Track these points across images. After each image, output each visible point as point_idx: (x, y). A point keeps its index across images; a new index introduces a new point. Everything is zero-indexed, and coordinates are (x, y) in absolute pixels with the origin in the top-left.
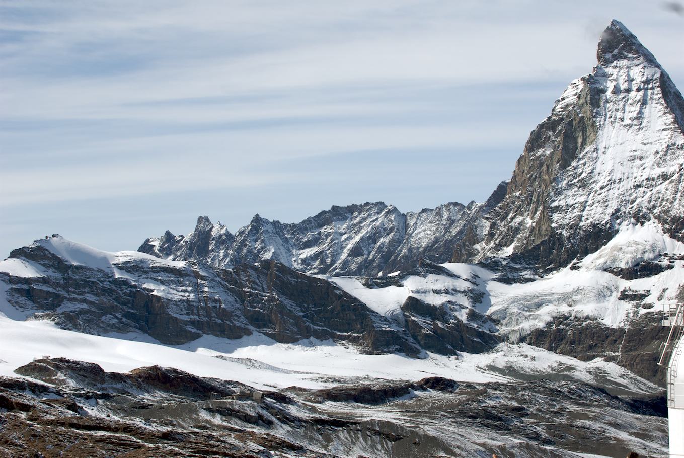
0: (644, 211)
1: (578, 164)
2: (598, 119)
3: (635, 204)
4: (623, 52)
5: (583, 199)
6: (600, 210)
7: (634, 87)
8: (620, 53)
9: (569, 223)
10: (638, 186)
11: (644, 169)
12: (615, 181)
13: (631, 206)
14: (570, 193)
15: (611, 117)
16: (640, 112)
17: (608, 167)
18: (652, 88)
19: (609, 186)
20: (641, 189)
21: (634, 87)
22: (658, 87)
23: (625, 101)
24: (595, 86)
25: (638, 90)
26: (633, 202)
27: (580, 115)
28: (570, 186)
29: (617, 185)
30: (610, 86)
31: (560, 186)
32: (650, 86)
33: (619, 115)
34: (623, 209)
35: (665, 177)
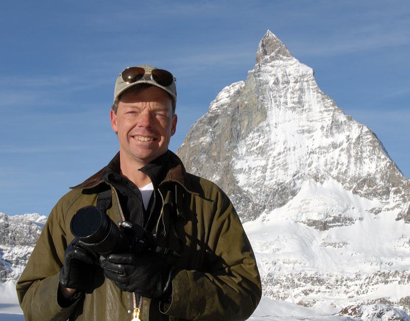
0: (322, 172)
5: (263, 163)
6: (281, 172)
7: (292, 81)
9: (255, 183)
10: (312, 152)
11: (314, 140)
12: (289, 149)
13: (309, 169)
14: (251, 158)
16: (300, 97)
17: (281, 138)
18: (307, 81)
19: (285, 152)
21: (292, 81)
25: (296, 82)
26: (310, 165)
27: (246, 102)
28: (249, 153)
30: (272, 80)
32: (305, 79)
33: (282, 100)
34: (302, 171)
35: (334, 146)
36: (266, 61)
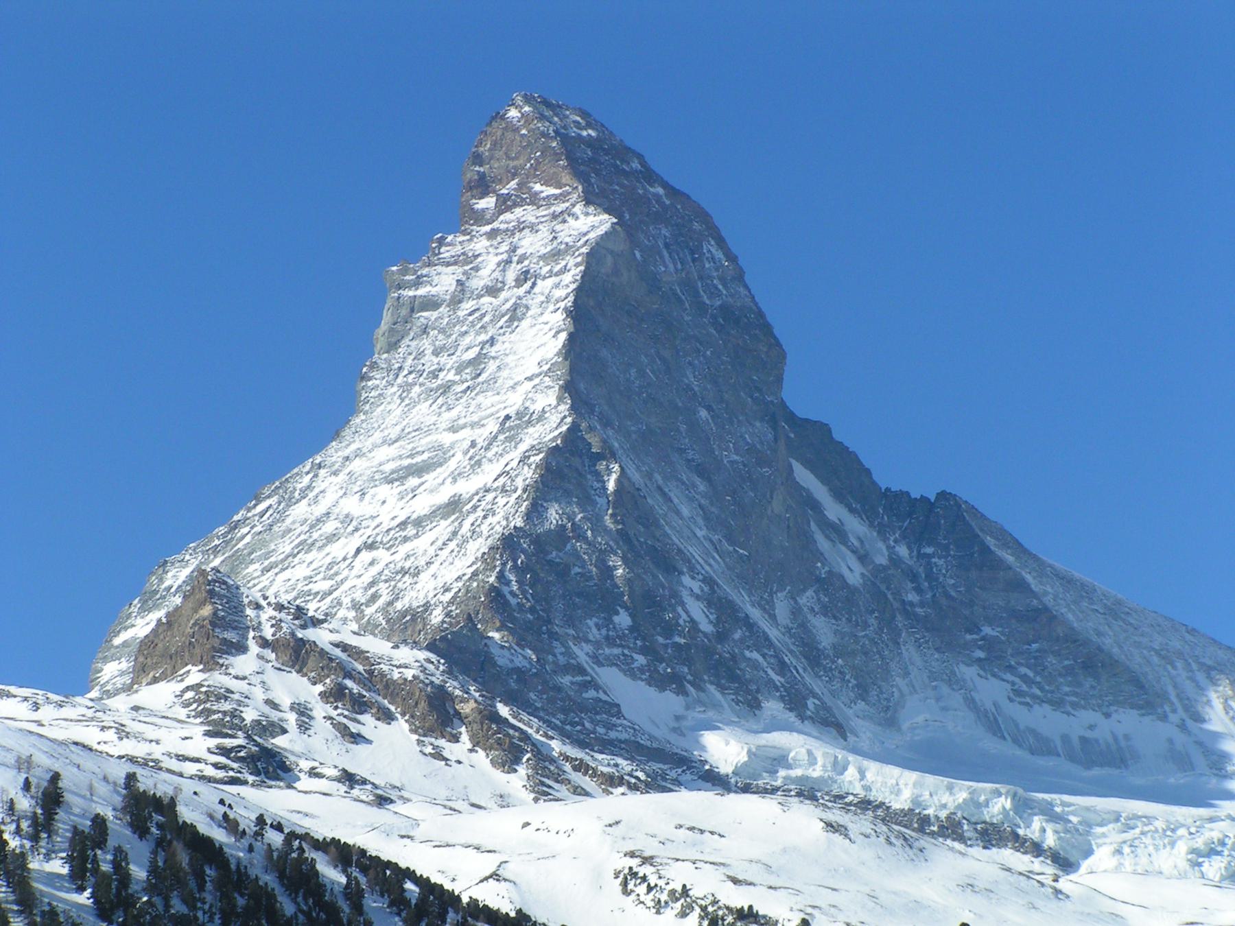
1: (249, 515)
2: (370, 383)
3: (329, 599)
4: (532, 185)
8: (521, 186)
10: (370, 546)
15: (410, 373)
16: (492, 342)
19: (290, 559)
20: (374, 554)
22: (577, 265)
23: (472, 322)
24: (411, 293)
25: (519, 282)
29: (313, 554)
31: (167, 584)
36: (480, 218)
